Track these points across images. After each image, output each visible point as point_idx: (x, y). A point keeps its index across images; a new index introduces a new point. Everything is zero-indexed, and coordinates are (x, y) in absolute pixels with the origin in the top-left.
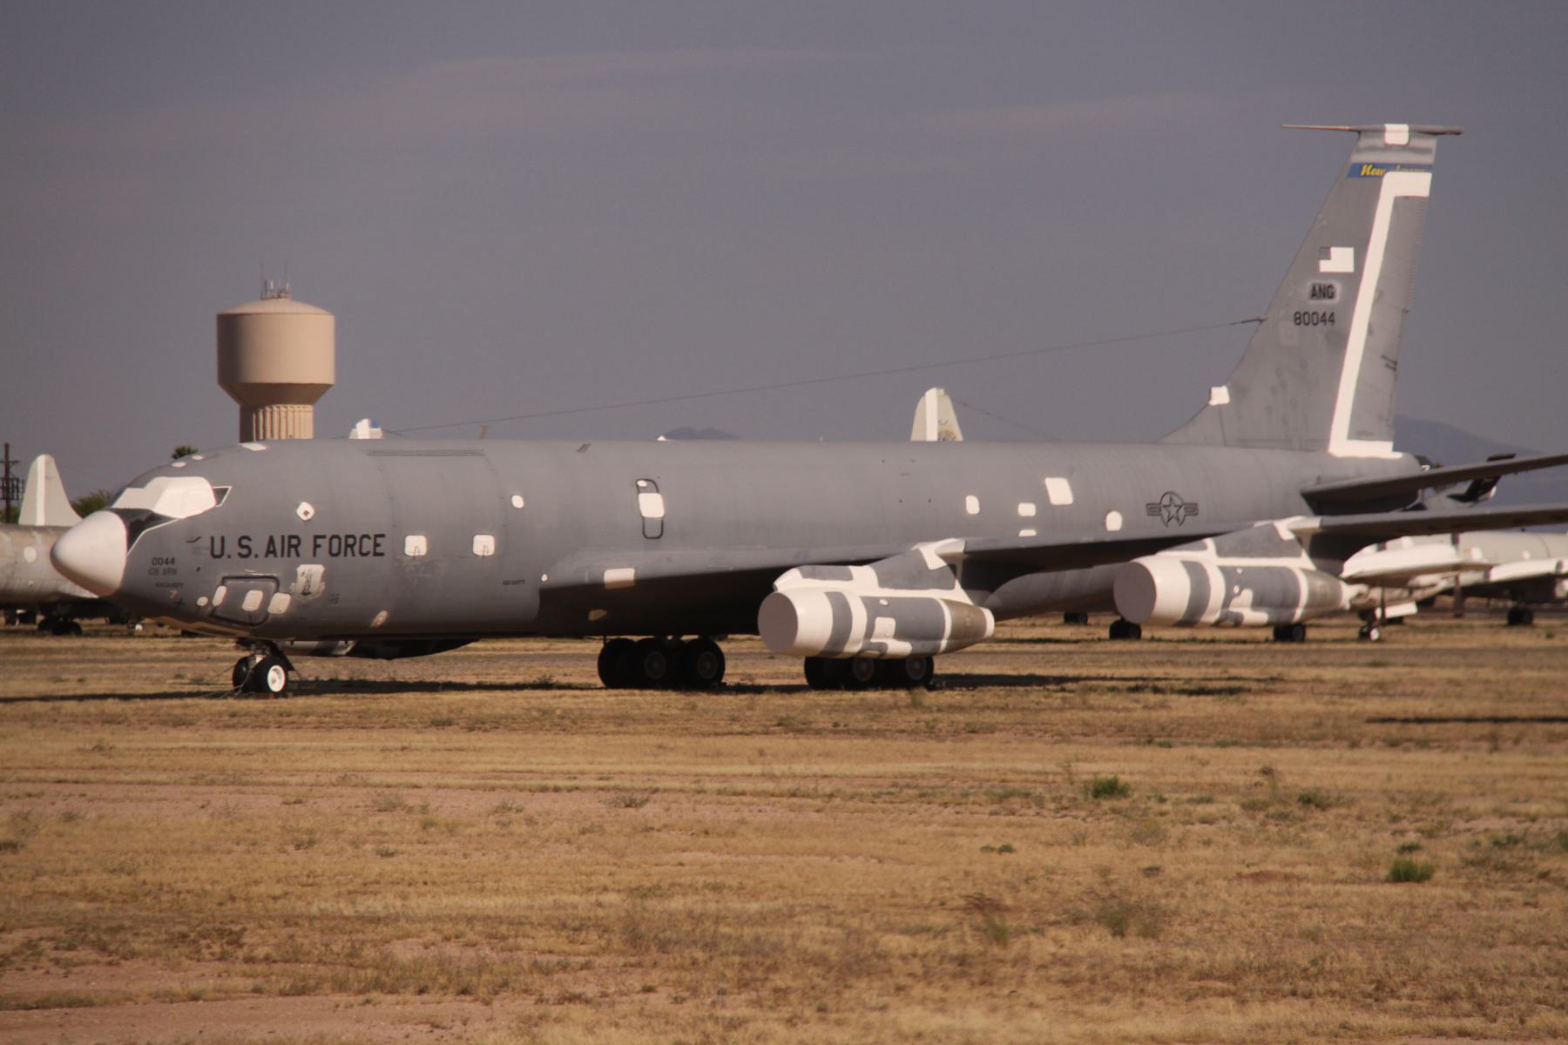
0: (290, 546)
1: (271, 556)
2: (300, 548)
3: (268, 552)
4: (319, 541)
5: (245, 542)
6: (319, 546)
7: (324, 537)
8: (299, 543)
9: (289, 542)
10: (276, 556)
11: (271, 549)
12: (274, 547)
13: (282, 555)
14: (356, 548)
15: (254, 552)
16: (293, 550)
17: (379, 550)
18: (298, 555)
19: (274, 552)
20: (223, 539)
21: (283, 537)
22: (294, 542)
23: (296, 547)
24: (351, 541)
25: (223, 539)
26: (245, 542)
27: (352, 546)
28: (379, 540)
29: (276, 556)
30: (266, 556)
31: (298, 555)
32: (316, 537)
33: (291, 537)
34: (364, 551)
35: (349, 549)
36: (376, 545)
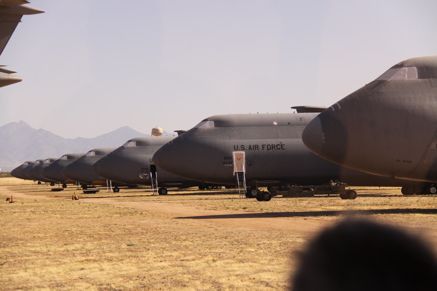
0: (256, 147)
1: (250, 150)
2: (258, 148)
3: (249, 149)
4: (264, 146)
5: (242, 147)
6: (264, 147)
7: (265, 145)
8: (258, 147)
9: (255, 147)
10: (252, 150)
11: (250, 148)
12: (251, 147)
13: (254, 149)
14: (276, 147)
15: (245, 149)
16: (256, 148)
17: (283, 148)
18: (258, 149)
19: (251, 149)
20: (237, 146)
21: (253, 145)
22: (257, 146)
23: (257, 147)
24: (274, 146)
25: (237, 146)
26: (242, 147)
27: (274, 147)
28: (282, 146)
29: (252, 150)
30: (249, 150)
31: (258, 149)
32: (263, 145)
33: (255, 145)
34: (278, 148)
35: (273, 148)
36: (282, 147)
